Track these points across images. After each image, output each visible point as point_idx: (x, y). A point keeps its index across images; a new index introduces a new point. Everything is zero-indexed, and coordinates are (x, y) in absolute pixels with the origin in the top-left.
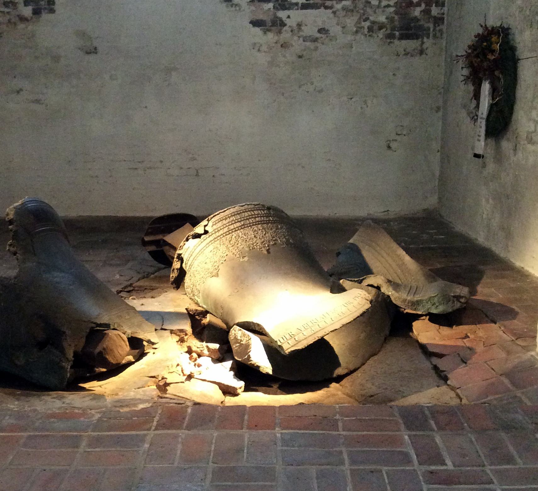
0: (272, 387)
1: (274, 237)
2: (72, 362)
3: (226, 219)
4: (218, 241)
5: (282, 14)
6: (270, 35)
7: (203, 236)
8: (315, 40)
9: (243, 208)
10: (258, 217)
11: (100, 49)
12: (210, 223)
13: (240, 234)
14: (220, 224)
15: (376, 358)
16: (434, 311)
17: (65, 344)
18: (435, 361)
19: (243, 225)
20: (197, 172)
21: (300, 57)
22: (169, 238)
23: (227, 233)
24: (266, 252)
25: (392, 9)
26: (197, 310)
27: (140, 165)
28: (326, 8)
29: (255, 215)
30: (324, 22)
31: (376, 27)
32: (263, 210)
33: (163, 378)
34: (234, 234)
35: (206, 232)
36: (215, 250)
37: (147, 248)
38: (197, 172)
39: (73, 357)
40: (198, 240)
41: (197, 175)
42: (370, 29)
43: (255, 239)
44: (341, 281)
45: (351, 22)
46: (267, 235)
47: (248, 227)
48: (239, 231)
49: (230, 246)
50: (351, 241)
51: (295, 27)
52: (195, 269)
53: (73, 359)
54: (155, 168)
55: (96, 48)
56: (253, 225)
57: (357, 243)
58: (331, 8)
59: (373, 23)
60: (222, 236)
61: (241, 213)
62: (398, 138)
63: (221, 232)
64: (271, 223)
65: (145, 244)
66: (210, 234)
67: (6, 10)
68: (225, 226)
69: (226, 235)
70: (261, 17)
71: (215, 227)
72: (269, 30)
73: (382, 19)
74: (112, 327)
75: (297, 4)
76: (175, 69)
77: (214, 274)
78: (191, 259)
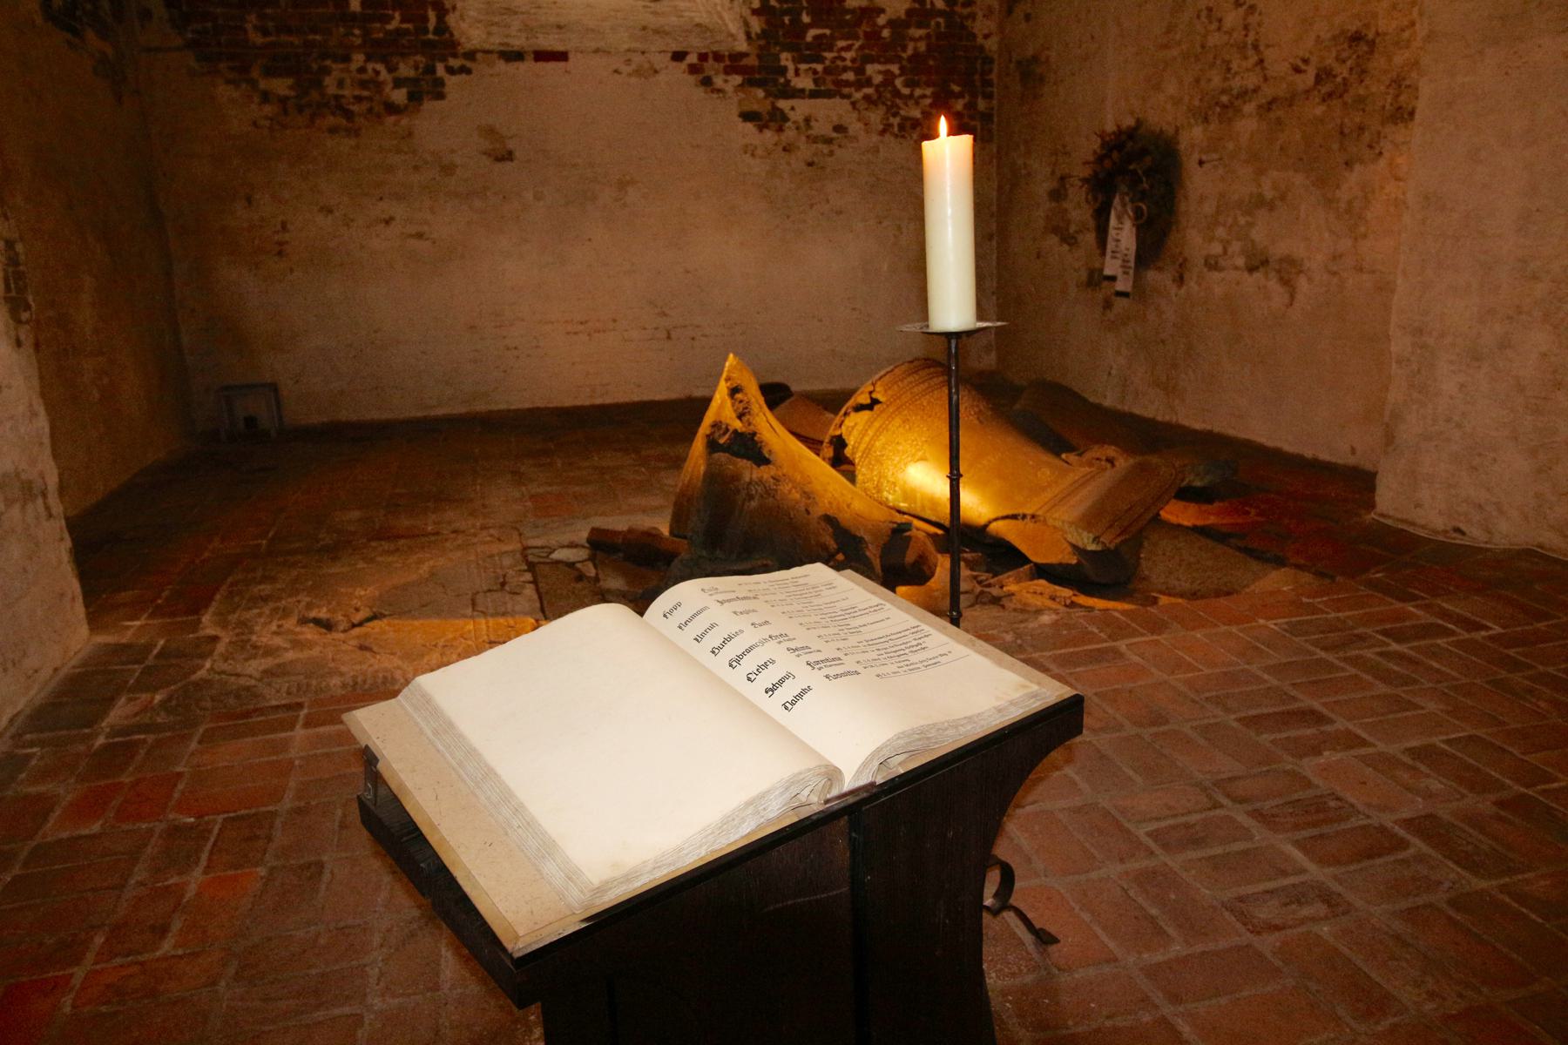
5: (783, 104)
6: (768, 134)
8: (829, 141)
11: (517, 154)
21: (810, 164)
25: (928, 101)
27: (581, 327)
28: (843, 97)
30: (841, 117)
31: (908, 124)
41: (669, 337)
42: (901, 127)
45: (876, 116)
51: (802, 124)
55: (510, 153)
58: (848, 96)
59: (905, 119)
67: (366, 93)
70: (755, 107)
72: (767, 127)
73: (916, 113)
75: (803, 90)
76: (632, 182)
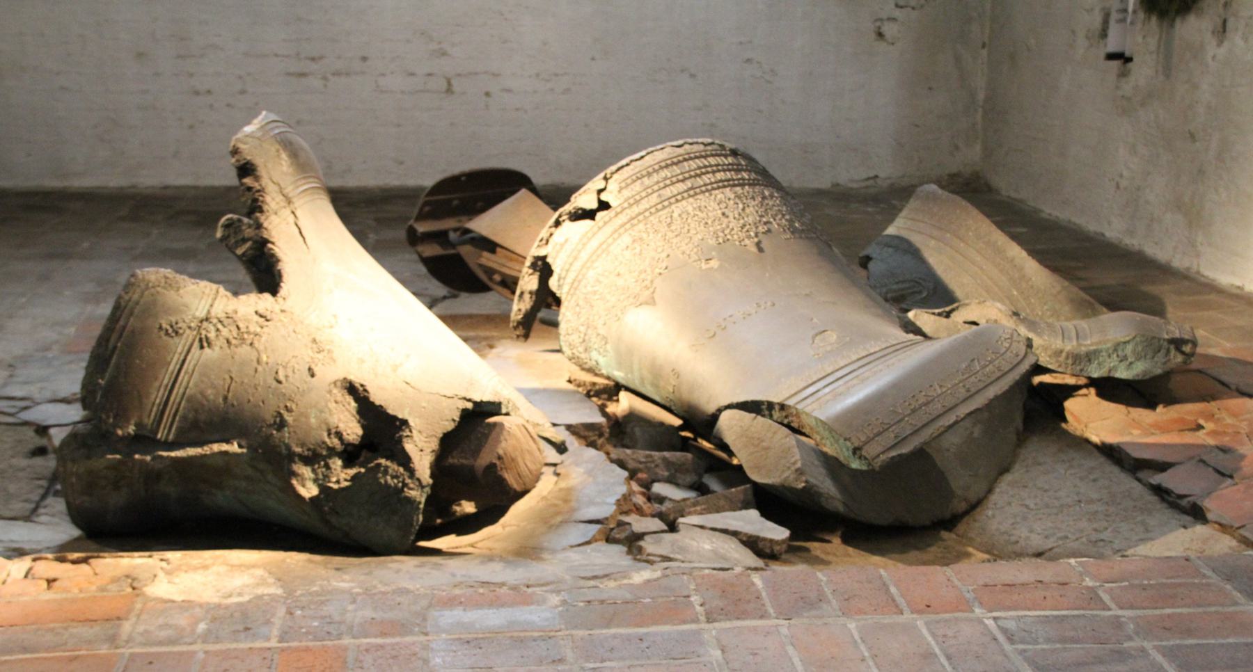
0: (828, 542)
1: (761, 216)
2: (428, 490)
3: (649, 174)
4: (641, 226)
7: (599, 215)
9: (681, 151)
10: (719, 171)
12: (613, 185)
13: (690, 209)
14: (637, 186)
15: (1008, 478)
16: (1122, 374)
17: (409, 447)
18: (1157, 479)
19: (692, 188)
20: (449, 83)
22: (483, 225)
23: (660, 206)
24: (754, 249)
26: (594, 384)
27: (314, 66)
29: (711, 166)
32: (726, 156)
33: (621, 524)
34: (677, 209)
35: (604, 206)
36: (636, 245)
37: (420, 248)
38: (449, 83)
39: (432, 476)
40: (586, 223)
41: (449, 90)
43: (726, 220)
44: (911, 315)
46: (747, 210)
47: (703, 192)
48: (684, 202)
49: (670, 235)
50: (891, 230)
52: (589, 289)
53: (431, 481)
54: (348, 74)
56: (714, 189)
57: (905, 234)
60: (647, 214)
61: (679, 162)
62: (897, 13)
63: (644, 205)
64: (750, 185)
65: (414, 239)
66: (619, 210)
68: (650, 191)
69: (658, 211)
71: (626, 193)
74: (504, 411)
77: (642, 299)
78: (577, 265)
